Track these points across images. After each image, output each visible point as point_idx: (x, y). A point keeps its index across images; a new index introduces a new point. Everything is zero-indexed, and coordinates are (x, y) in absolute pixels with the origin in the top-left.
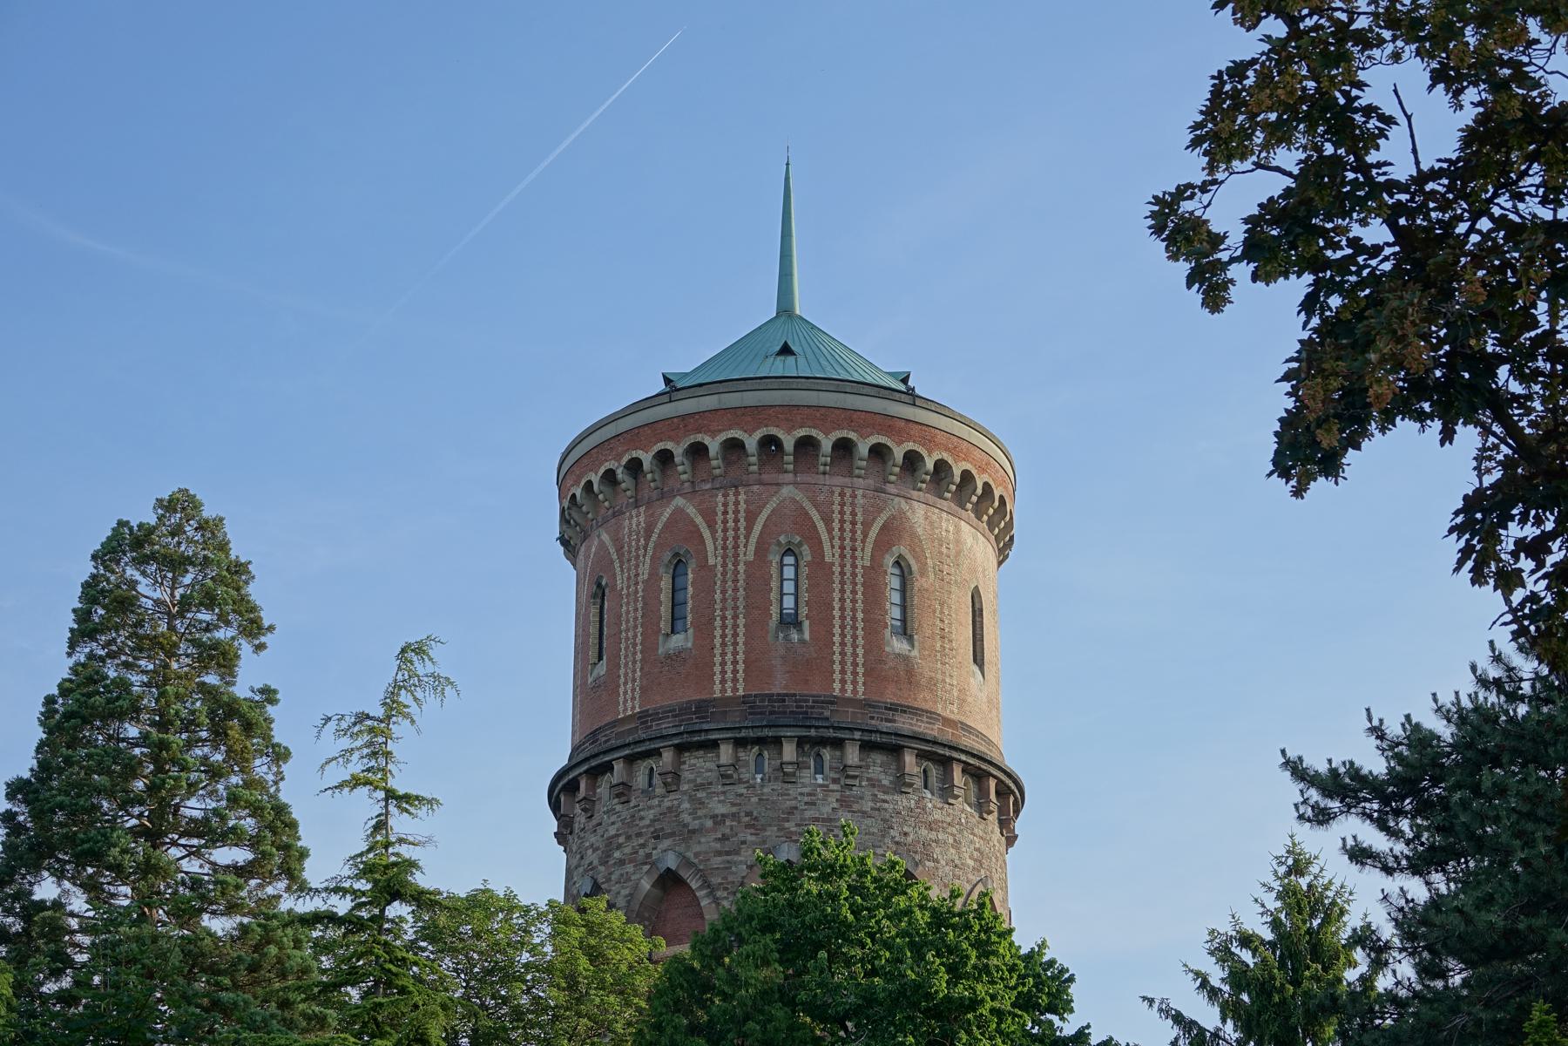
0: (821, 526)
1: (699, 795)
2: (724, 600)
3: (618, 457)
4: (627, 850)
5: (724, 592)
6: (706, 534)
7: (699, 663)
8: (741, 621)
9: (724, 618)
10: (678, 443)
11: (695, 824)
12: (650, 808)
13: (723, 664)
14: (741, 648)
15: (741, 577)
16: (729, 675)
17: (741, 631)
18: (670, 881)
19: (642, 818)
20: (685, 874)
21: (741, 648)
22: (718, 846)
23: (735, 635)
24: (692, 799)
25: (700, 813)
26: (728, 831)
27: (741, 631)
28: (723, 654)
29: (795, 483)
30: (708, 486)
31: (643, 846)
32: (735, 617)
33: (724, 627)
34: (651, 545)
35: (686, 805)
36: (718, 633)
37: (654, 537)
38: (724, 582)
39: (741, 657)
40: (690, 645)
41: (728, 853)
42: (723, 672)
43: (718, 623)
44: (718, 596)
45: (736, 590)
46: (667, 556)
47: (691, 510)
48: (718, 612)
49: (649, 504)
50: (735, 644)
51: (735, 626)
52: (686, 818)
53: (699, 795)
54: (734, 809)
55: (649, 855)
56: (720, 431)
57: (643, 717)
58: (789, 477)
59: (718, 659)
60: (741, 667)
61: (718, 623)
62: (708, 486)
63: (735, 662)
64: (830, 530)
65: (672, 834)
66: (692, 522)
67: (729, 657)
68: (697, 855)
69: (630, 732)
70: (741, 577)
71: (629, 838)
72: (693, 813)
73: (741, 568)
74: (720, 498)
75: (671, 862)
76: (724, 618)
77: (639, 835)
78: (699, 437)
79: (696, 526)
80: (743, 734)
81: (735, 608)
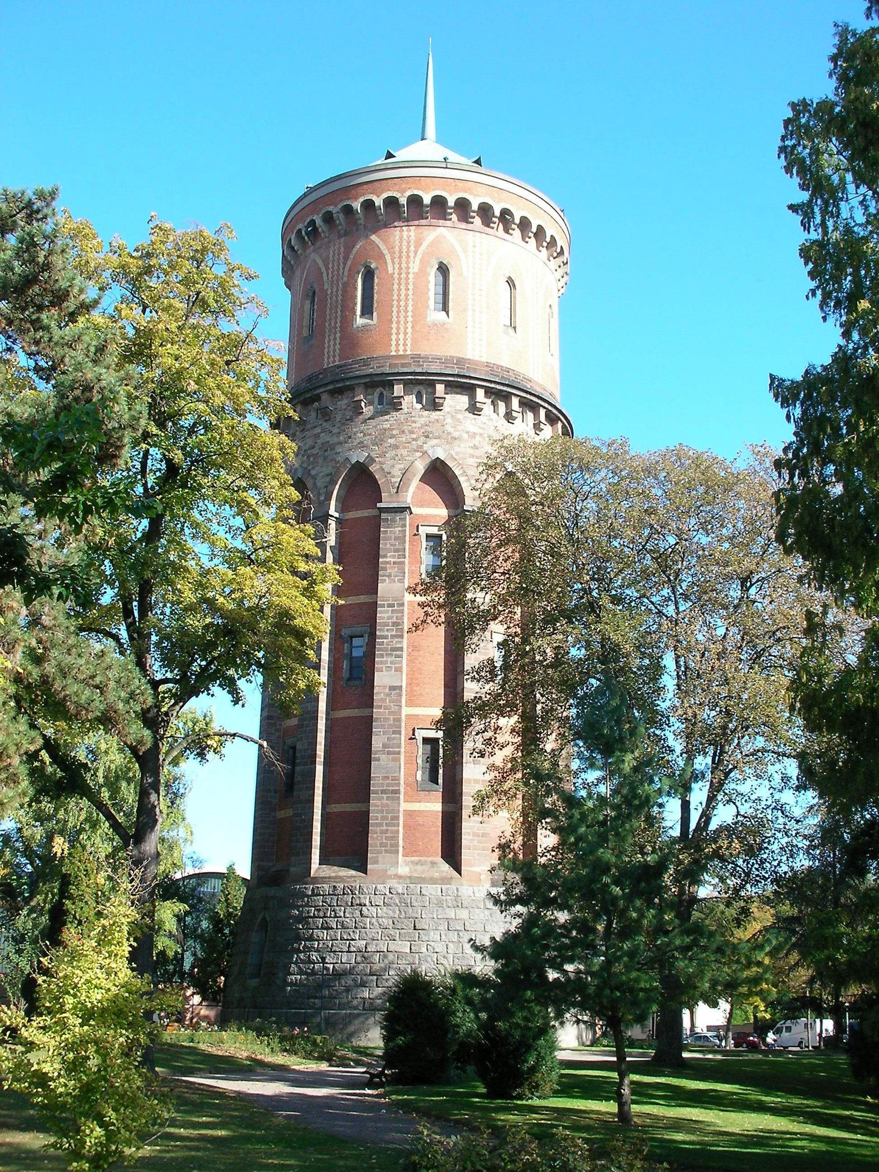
3: (403, 191)
10: (451, 195)
11: (456, 434)
22: (471, 451)
26: (477, 444)
54: (481, 431)
65: (439, 437)
68: (457, 453)
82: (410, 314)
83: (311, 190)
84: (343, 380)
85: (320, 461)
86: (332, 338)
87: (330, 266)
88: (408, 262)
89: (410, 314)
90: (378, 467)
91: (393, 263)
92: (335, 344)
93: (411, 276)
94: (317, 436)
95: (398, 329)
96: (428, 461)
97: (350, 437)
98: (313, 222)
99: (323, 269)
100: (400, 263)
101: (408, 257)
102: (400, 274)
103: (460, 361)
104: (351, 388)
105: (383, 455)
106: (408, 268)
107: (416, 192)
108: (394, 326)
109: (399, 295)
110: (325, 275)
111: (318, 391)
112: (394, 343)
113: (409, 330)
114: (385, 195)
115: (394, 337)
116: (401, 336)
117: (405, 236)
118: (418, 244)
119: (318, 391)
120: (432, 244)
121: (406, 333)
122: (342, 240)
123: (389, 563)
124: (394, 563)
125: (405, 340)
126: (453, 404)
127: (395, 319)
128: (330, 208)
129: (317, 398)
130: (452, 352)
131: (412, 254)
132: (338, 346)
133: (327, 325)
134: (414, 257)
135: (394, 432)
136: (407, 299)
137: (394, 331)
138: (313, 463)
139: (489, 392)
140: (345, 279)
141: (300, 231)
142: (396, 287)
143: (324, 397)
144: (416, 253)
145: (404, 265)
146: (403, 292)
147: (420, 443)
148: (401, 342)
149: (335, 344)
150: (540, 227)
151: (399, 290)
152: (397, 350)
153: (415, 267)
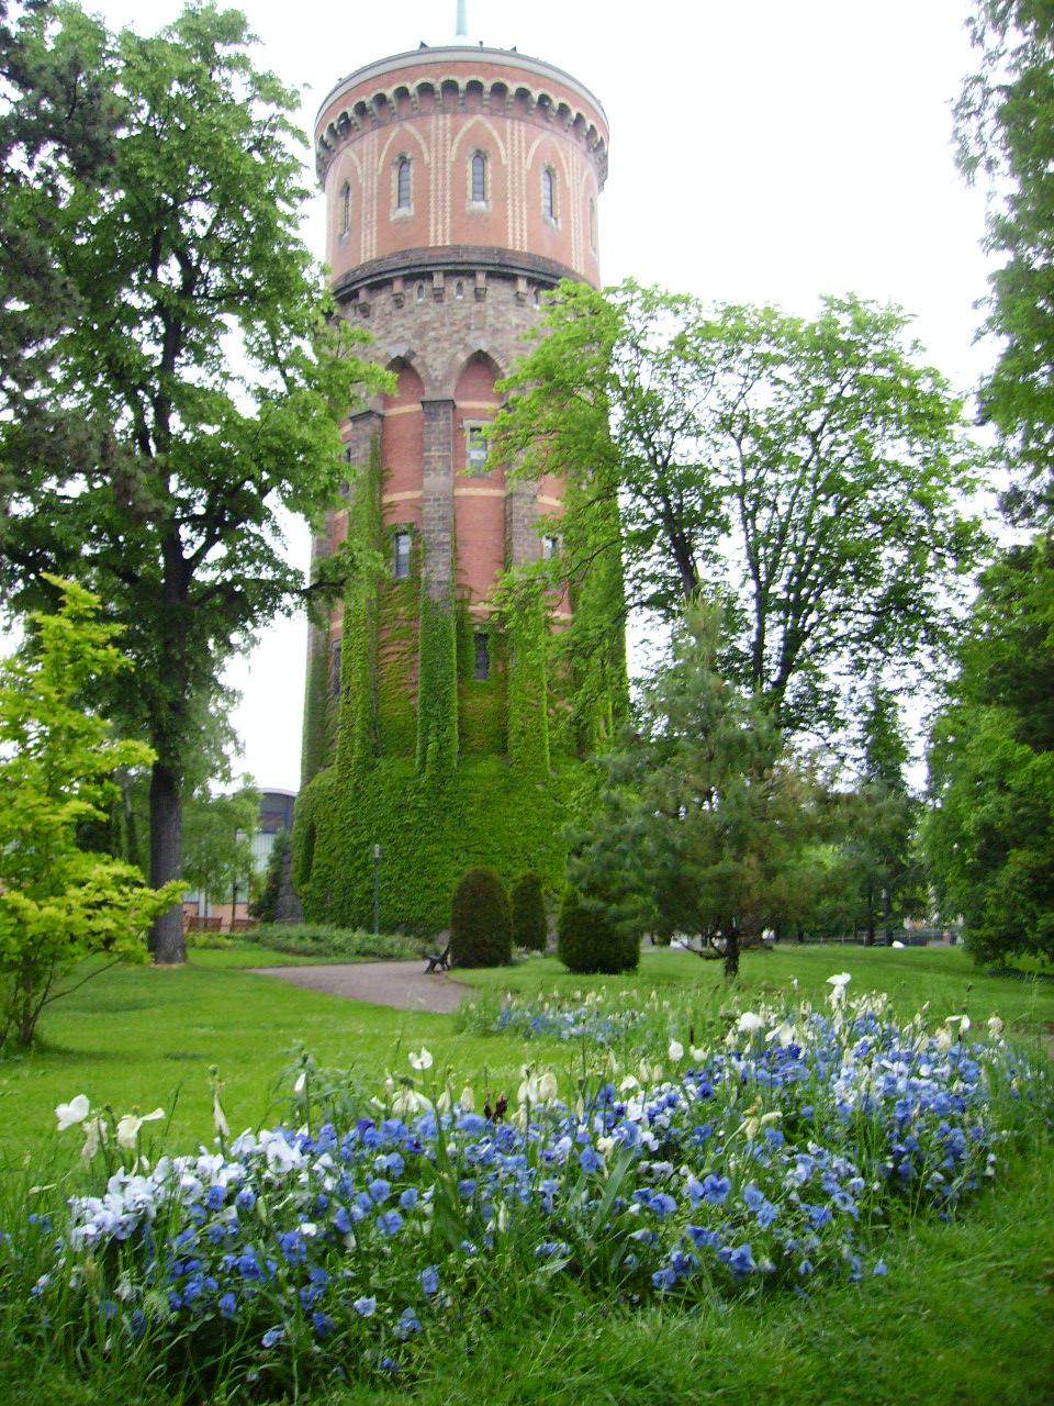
1: (502, 308)
3: (437, 77)
4: (445, 331)
8: (525, 205)
11: (499, 326)
20: (494, 356)
24: (495, 308)
34: (457, 140)
35: (491, 312)
40: (490, 209)
46: (472, 151)
47: (489, 125)
55: (462, 339)
57: (455, 249)
71: (443, 325)
75: (483, 346)
77: (453, 324)
78: (502, 80)
83: (342, 82)
84: (380, 274)
96: (470, 353)
98: (345, 114)
103: (502, 252)
104: (389, 282)
105: (424, 348)
107: (451, 78)
108: (432, 216)
113: (448, 220)
114: (419, 82)
115: (432, 229)
118: (455, 131)
120: (471, 130)
127: (432, 210)
128: (363, 99)
129: (355, 294)
130: (493, 242)
137: (432, 221)
139: (531, 282)
142: (432, 177)
143: (363, 294)
145: (440, 155)
147: (462, 335)
150: (579, 116)
153: (452, 155)
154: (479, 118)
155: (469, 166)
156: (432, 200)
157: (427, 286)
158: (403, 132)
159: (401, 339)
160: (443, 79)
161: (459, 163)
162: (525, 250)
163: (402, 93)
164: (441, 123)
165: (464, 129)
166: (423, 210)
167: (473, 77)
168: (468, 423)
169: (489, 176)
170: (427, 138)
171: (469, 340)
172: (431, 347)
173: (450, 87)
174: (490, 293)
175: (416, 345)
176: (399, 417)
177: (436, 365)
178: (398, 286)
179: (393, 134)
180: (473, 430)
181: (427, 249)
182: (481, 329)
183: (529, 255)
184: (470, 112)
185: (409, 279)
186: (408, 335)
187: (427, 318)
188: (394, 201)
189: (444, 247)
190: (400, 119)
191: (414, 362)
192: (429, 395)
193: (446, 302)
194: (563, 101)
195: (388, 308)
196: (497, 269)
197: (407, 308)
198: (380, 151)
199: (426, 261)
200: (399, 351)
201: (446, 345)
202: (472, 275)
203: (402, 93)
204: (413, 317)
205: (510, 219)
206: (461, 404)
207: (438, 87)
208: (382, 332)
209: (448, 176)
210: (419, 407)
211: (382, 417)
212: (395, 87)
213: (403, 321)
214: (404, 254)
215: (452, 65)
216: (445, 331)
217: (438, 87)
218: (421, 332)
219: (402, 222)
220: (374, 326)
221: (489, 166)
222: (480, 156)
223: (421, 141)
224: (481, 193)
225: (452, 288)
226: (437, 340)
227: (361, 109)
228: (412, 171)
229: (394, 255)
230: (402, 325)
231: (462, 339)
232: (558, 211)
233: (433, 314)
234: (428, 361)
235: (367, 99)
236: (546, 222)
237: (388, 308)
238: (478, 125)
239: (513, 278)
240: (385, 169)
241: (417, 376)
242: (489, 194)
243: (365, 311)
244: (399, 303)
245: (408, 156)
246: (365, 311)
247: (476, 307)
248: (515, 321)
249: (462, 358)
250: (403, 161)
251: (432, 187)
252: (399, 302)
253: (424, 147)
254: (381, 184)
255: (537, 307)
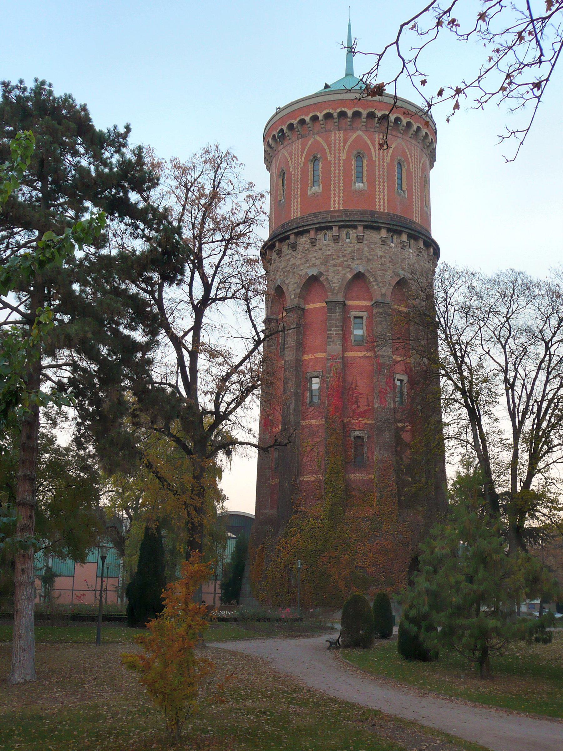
0: (409, 156)
1: (371, 246)
2: (379, 175)
3: (335, 109)
4: (339, 261)
5: (379, 172)
6: (372, 148)
7: (370, 195)
9: (379, 182)
10: (364, 110)
11: (371, 257)
12: (349, 247)
13: (380, 199)
14: (386, 194)
15: (385, 167)
16: (382, 203)
17: (386, 188)
18: (359, 277)
19: (345, 250)
21: (386, 194)
23: (384, 189)
25: (372, 253)
27: (386, 188)
28: (380, 195)
29: (402, 138)
30: (373, 130)
31: (347, 261)
32: (384, 182)
33: (379, 185)
35: (366, 249)
36: (377, 186)
37: (348, 144)
38: (379, 168)
39: (386, 198)
40: (366, 188)
41: (383, 270)
42: (380, 202)
43: (377, 183)
44: (377, 173)
45: (384, 172)
46: (355, 152)
47: (365, 137)
48: (377, 179)
49: (345, 130)
50: (384, 192)
51: (384, 186)
52: (368, 254)
53: (371, 246)
54: (385, 254)
56: (381, 110)
57: (345, 212)
58: (400, 135)
59: (377, 196)
60: (386, 201)
61: (377, 183)
62: (373, 130)
63: (384, 199)
64: (412, 159)
66: (366, 142)
67: (382, 197)
68: (371, 268)
69: (339, 216)
70: (385, 167)
71: (338, 257)
72: (369, 252)
73: (385, 164)
74: (377, 136)
76: (379, 182)
77: (344, 256)
79: (368, 144)
80: (392, 227)
81: (384, 179)
82: (341, 185)
83: (280, 110)
84: (303, 226)
85: (291, 274)
86: (295, 201)
87: (293, 157)
88: (339, 153)
89: (341, 185)
90: (325, 277)
91: (331, 154)
92: (297, 205)
93: (342, 162)
94: (288, 260)
95: (335, 194)
97: (308, 261)
98: (282, 130)
99: (289, 159)
100: (335, 154)
101: (339, 150)
102: (335, 161)
103: (372, 213)
104: (308, 231)
106: (339, 157)
108: (332, 192)
109: (335, 173)
110: (290, 162)
111: (288, 233)
112: (332, 203)
113: (341, 195)
114: (325, 112)
115: (332, 199)
116: (337, 198)
117: (337, 137)
118: (345, 141)
119: (288, 233)
120: (354, 141)
121: (339, 197)
122: (300, 140)
123: (333, 334)
124: (336, 334)
125: (339, 201)
126: (368, 239)
127: (332, 188)
128: (292, 121)
129: (288, 237)
131: (342, 148)
132: (299, 206)
133: (292, 193)
134: (343, 150)
135: (334, 257)
136: (339, 176)
137: (332, 195)
138: (286, 276)
139: (389, 230)
140: (302, 165)
141: (274, 136)
142: (333, 168)
143: (292, 237)
144: (344, 147)
145: (337, 155)
146: (337, 172)
148: (337, 202)
149: (297, 205)
151: (335, 170)
152: (334, 207)
153: (344, 156)
154: (359, 133)
155: (353, 162)
156: (332, 183)
157: (329, 234)
158: (316, 141)
159: (314, 265)
160: (338, 111)
161: (348, 160)
162: (386, 211)
163: (315, 118)
164: (337, 136)
165: (350, 141)
166: (327, 187)
167: (356, 109)
168: (353, 313)
169: (365, 168)
170: (329, 145)
171: (354, 266)
172: (332, 269)
173: (343, 114)
174: (366, 237)
175: (323, 268)
176: (313, 309)
177: (334, 280)
178: (312, 233)
179: (310, 143)
180: (355, 317)
181: (330, 212)
182: (361, 259)
183: (388, 214)
184: (353, 129)
185: (318, 230)
186: (318, 262)
187: (329, 253)
188: (310, 183)
189: (339, 211)
190: (313, 134)
191: (321, 279)
192: (331, 298)
193: (340, 243)
194: (408, 120)
195: (307, 246)
196: (370, 224)
197: (317, 247)
198: (302, 152)
199: (329, 220)
200: (314, 272)
201: (340, 268)
202: (355, 227)
203: (315, 118)
204: (320, 252)
205: (377, 193)
206: (349, 303)
207: (335, 115)
208: (303, 260)
209: (342, 168)
210: (324, 304)
211: (303, 310)
212: (311, 115)
213: (315, 254)
214: (316, 215)
215: (342, 102)
216: (339, 261)
217: (335, 115)
218: (325, 261)
219: (315, 195)
220: (299, 256)
221: (365, 162)
222: (359, 156)
223: (326, 147)
224: (359, 178)
225: (343, 234)
226: (335, 266)
227: (291, 127)
228: (321, 165)
229: (310, 215)
230: (315, 257)
231: (350, 265)
232: (404, 186)
233: (332, 250)
234: (330, 278)
235: (295, 122)
236: (399, 194)
237: (307, 246)
238: (359, 137)
239: (378, 229)
240: (305, 164)
241: (324, 286)
242: (365, 179)
243: (294, 247)
244: (313, 243)
245: (319, 156)
246: (294, 247)
247: (357, 247)
248: (380, 254)
249: (349, 276)
250: (315, 159)
251: (332, 175)
252: (313, 243)
253: (328, 151)
254: (302, 171)
255: (393, 245)
